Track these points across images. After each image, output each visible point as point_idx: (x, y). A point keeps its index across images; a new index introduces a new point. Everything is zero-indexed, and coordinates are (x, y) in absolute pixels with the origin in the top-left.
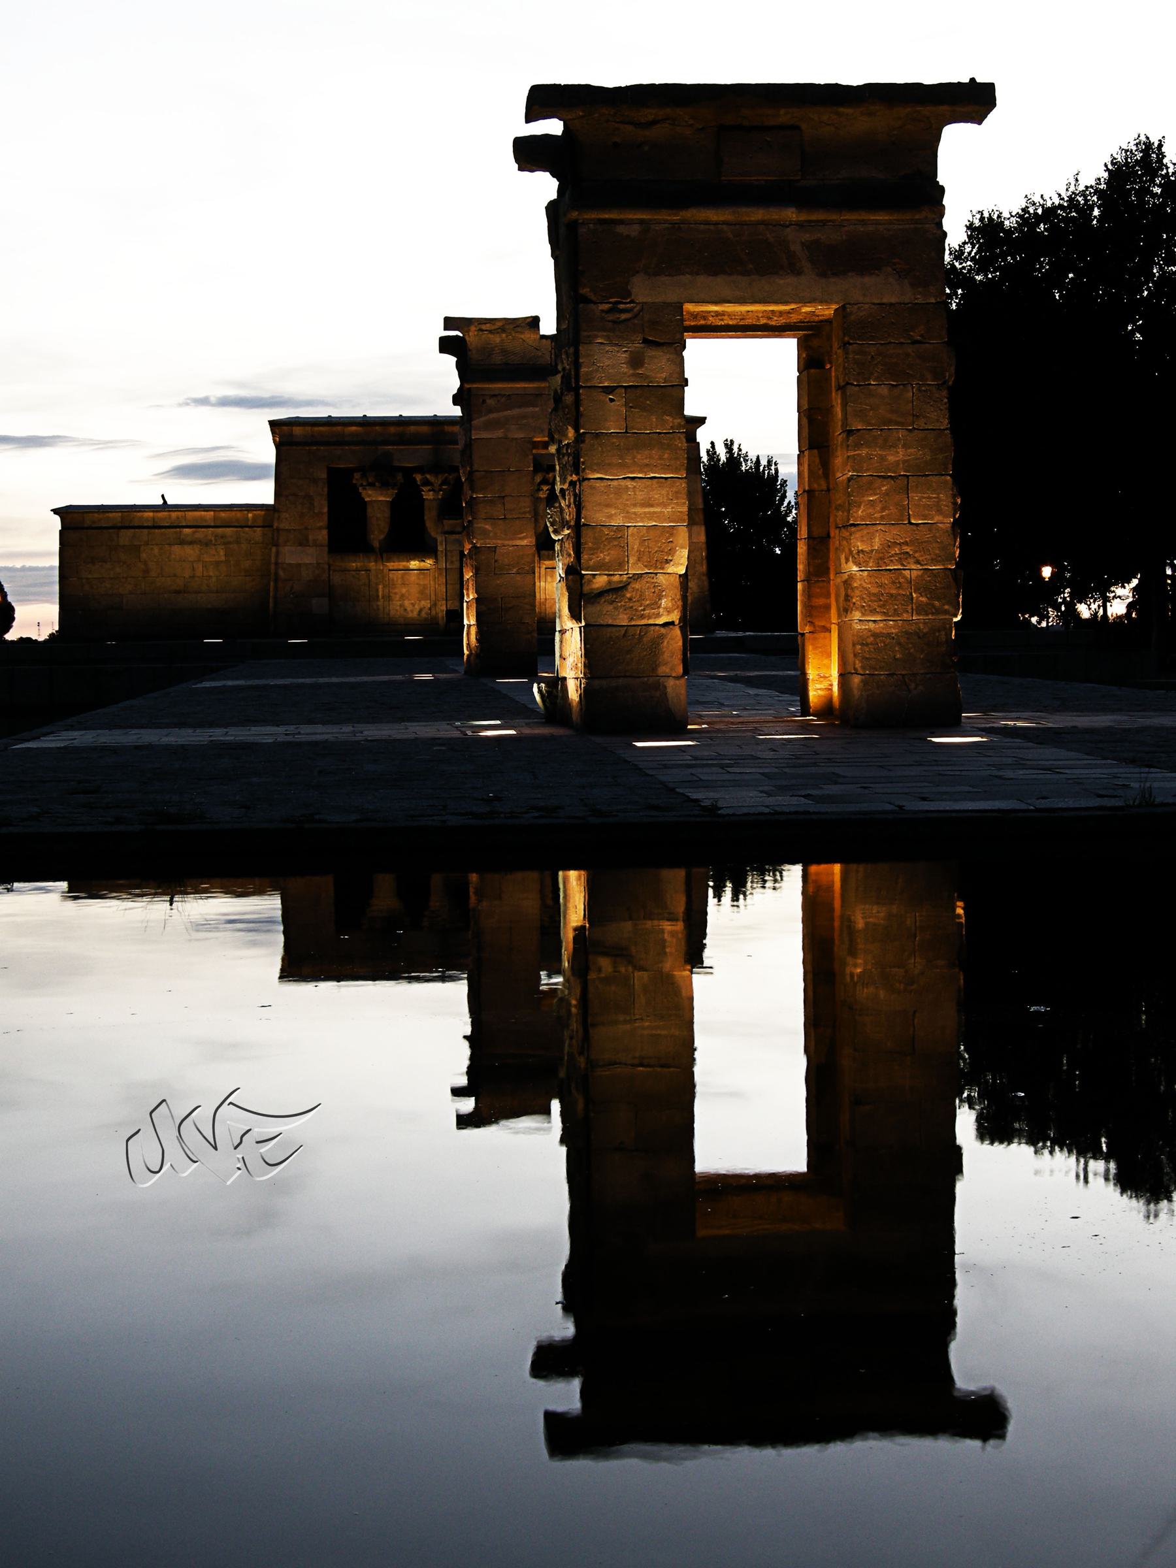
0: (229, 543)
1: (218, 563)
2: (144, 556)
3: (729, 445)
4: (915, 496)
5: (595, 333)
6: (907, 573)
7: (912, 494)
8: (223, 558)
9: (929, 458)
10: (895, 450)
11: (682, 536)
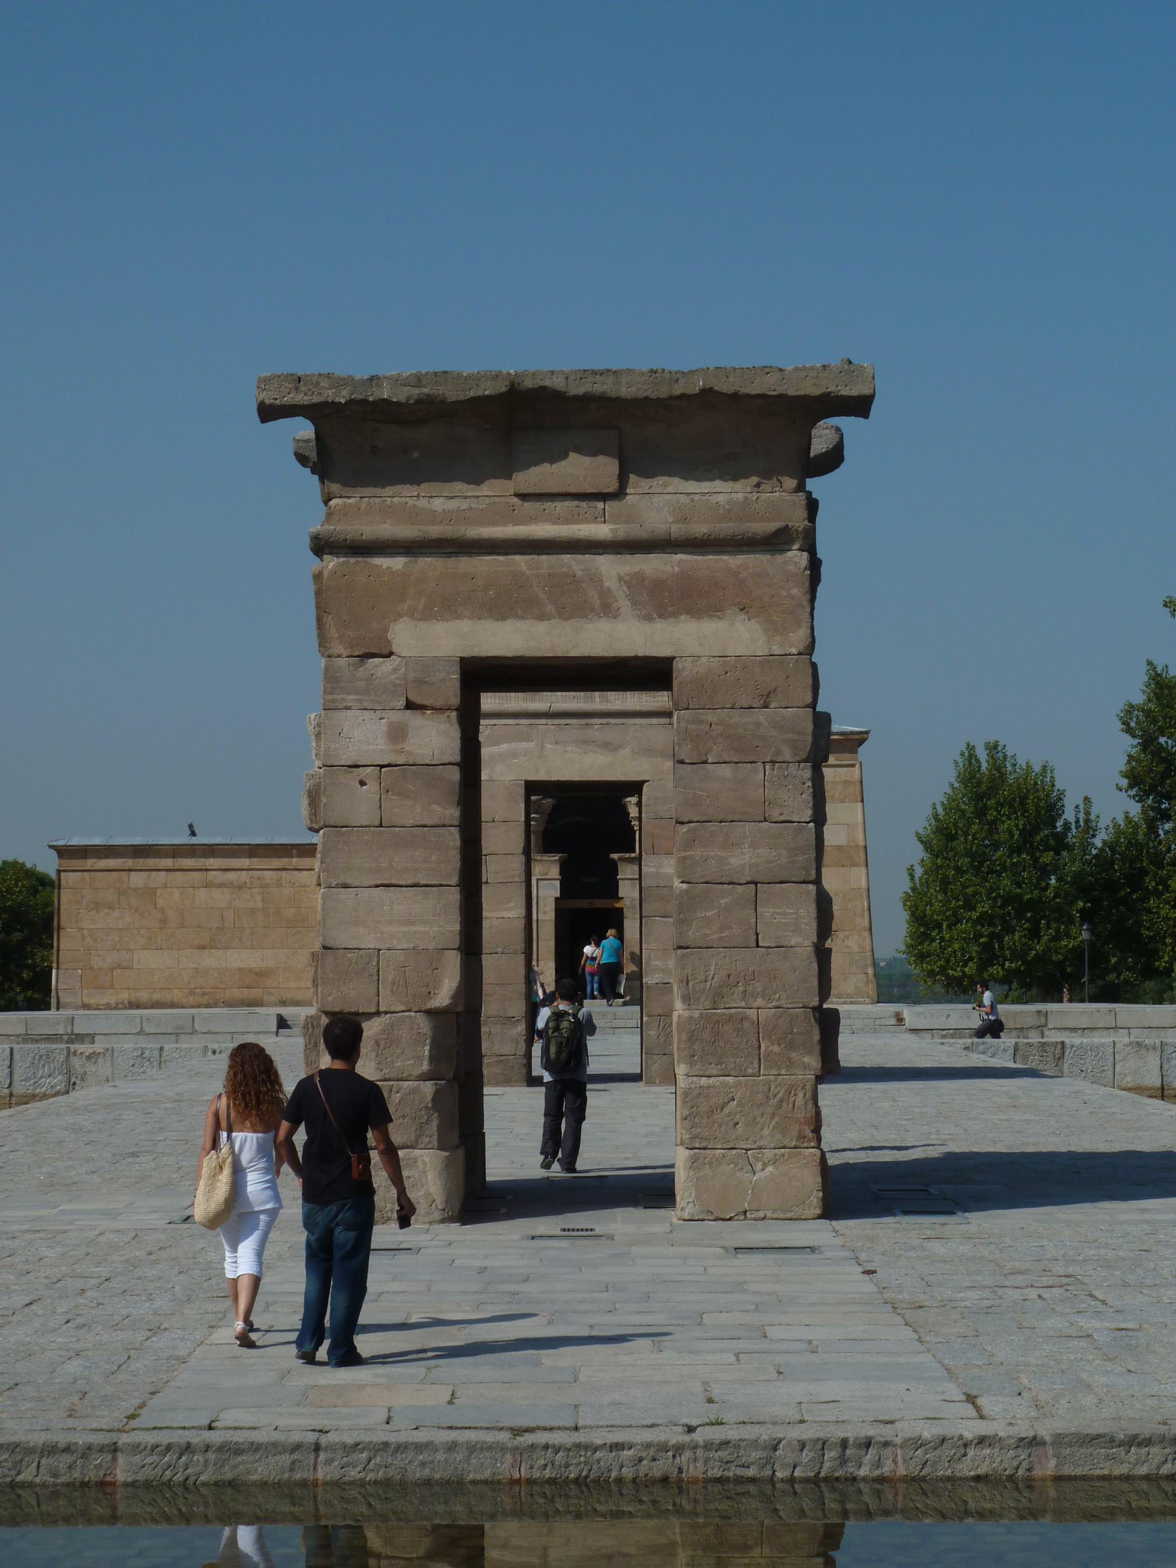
0: (267, 886)
1: (253, 911)
2: (161, 902)
3: (993, 748)
4: (765, 911)
5: (346, 697)
6: (752, 1013)
7: (761, 910)
8: (260, 905)
9: (784, 860)
10: (740, 850)
11: (452, 964)
